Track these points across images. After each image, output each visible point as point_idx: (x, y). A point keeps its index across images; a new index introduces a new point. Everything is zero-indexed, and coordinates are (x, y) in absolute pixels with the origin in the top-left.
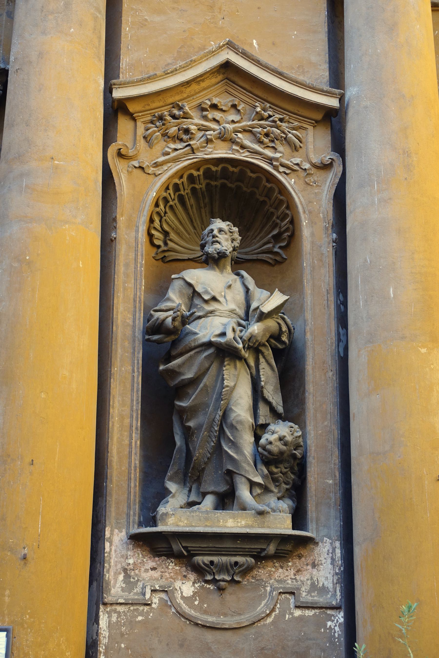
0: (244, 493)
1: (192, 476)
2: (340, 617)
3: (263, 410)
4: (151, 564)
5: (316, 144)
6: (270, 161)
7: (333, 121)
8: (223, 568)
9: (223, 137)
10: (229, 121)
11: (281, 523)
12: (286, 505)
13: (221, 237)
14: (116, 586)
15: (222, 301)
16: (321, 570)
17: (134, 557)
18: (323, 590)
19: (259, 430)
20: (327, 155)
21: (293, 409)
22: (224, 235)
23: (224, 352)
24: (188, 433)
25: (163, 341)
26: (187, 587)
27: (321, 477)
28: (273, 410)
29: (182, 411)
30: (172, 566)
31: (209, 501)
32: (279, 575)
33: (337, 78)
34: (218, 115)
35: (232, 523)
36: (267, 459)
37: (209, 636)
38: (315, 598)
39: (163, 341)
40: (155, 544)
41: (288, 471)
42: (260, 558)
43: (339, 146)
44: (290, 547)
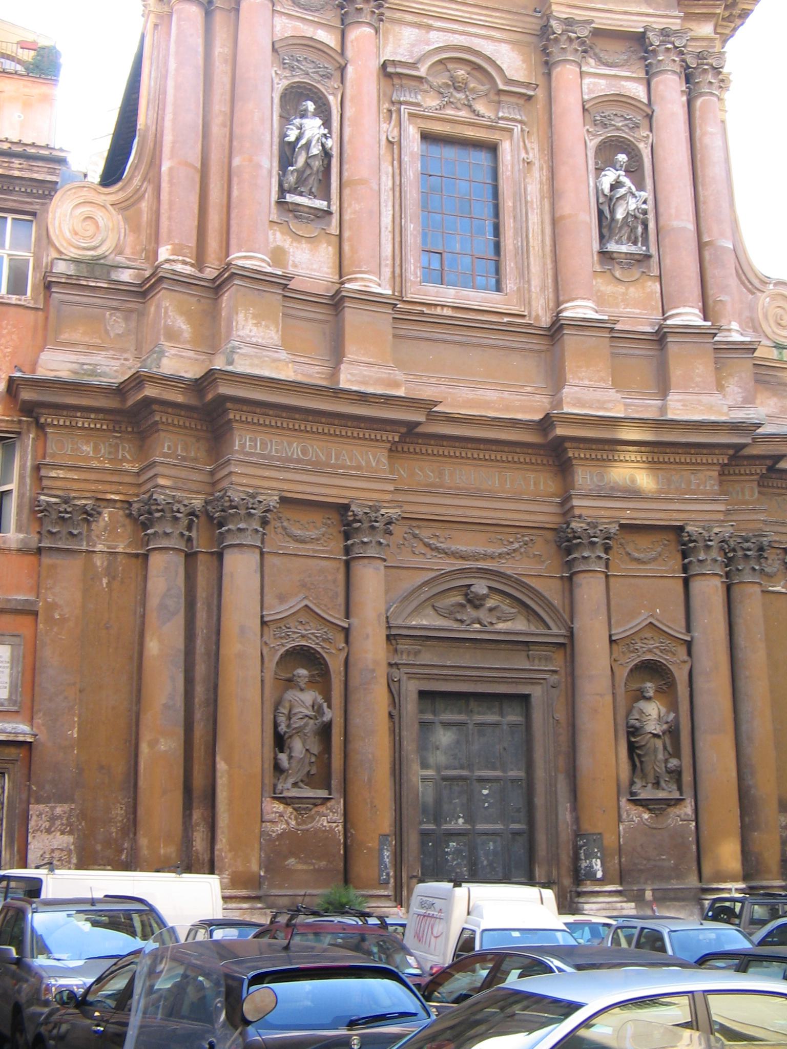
0: (663, 784)
1: (644, 776)
2: (694, 824)
3: (666, 753)
4: (634, 808)
5: (682, 652)
6: (666, 660)
7: (689, 645)
8: (658, 809)
9: (650, 651)
10: (652, 644)
11: (676, 795)
12: (675, 787)
13: (650, 690)
14: (624, 816)
15: (653, 714)
16: (688, 809)
17: (629, 807)
18: (688, 815)
19: (666, 761)
20: (686, 658)
21: (677, 754)
22: (650, 687)
23: (656, 736)
24: (641, 762)
25: (633, 732)
26: (646, 816)
27: (687, 778)
28: (669, 754)
29: (639, 756)
30: (641, 809)
31: (650, 785)
32: (674, 811)
33: (688, 629)
34: (646, 641)
35: (661, 795)
36: (669, 772)
37: (654, 831)
38: (686, 818)
39: (633, 732)
40: (636, 802)
41: (676, 775)
42: (669, 805)
43: (689, 653)
44: (679, 801)
